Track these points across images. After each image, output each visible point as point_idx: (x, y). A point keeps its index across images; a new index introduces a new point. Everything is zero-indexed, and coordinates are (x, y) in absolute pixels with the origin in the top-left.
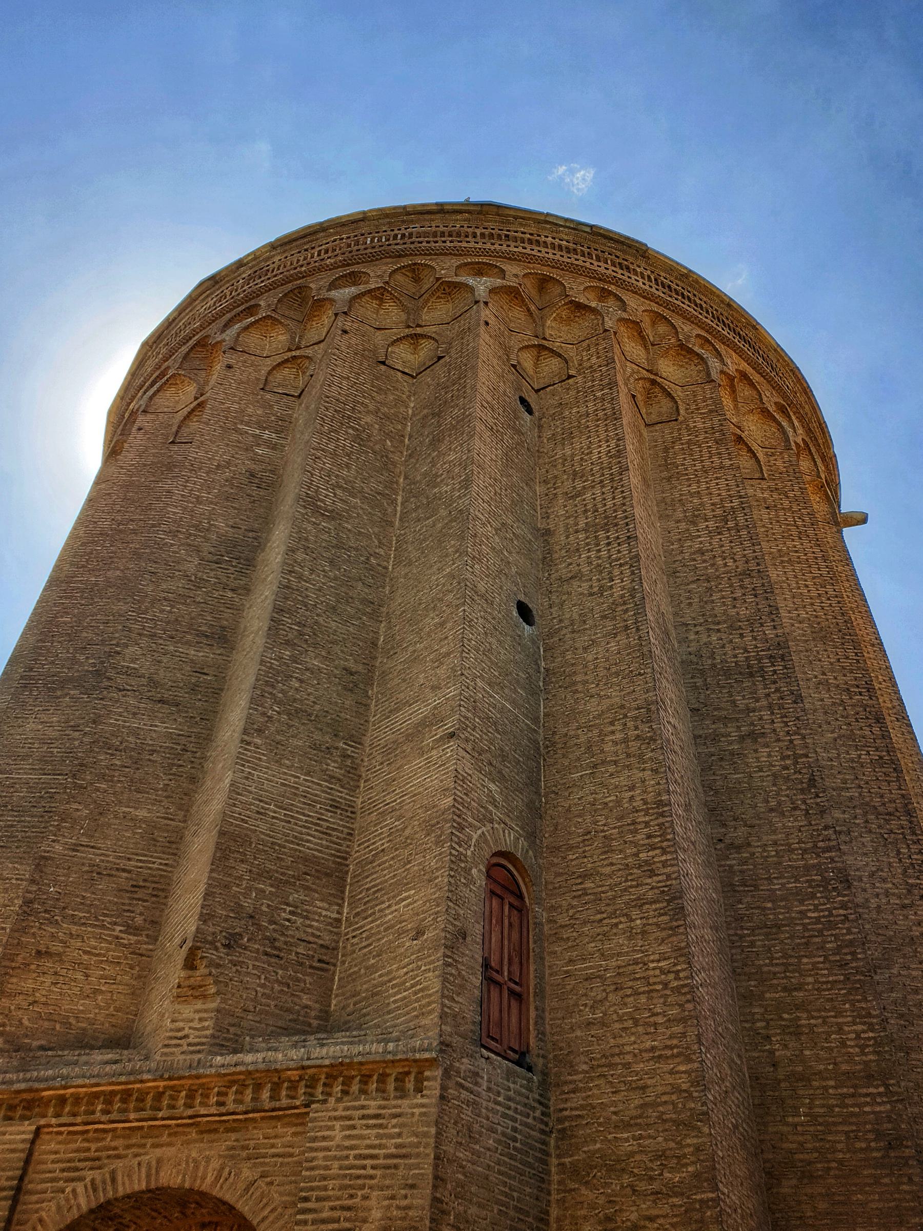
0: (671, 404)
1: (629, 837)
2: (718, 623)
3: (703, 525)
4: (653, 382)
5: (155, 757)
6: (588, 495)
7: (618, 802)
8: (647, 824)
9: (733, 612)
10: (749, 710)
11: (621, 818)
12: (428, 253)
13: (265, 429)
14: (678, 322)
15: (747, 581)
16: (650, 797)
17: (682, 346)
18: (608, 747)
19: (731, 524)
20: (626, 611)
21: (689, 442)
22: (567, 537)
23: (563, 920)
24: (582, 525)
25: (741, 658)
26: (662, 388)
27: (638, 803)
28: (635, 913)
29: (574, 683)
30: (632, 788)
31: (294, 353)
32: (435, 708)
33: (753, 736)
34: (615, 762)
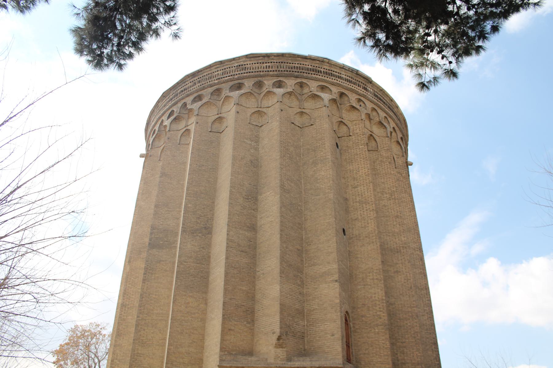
0: (375, 143)
1: (374, 308)
2: (389, 233)
3: (385, 196)
4: (371, 135)
5: (244, 270)
6: (359, 188)
7: (371, 297)
8: (379, 305)
9: (393, 230)
10: (397, 264)
11: (372, 302)
12: (306, 78)
13: (252, 141)
14: (379, 111)
15: (397, 219)
16: (380, 297)
17: (380, 122)
18: (368, 280)
19: (393, 197)
20: (373, 236)
21: (381, 161)
22: (353, 203)
24: (358, 200)
25: (395, 246)
26: (374, 138)
28: (376, 328)
29: (357, 258)
30: (375, 294)
31: (259, 109)
33: (397, 272)
34: (370, 285)
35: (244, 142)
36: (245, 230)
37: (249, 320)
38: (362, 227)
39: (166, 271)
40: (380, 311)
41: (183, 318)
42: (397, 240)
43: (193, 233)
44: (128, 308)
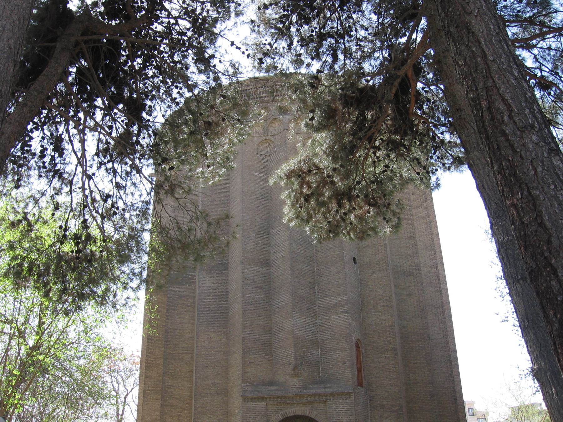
5: (260, 305)
7: (382, 323)
8: (389, 331)
9: (406, 252)
10: (409, 286)
18: (379, 307)
20: (383, 263)
23: (369, 353)
25: (408, 269)
27: (387, 325)
28: (386, 353)
30: (385, 320)
31: (266, 137)
32: (339, 301)
33: (410, 295)
35: (253, 175)
36: (259, 266)
37: (268, 352)
38: (373, 255)
39: (188, 306)
40: (390, 337)
41: (207, 353)
42: (410, 262)
43: (211, 270)
44: (154, 341)
